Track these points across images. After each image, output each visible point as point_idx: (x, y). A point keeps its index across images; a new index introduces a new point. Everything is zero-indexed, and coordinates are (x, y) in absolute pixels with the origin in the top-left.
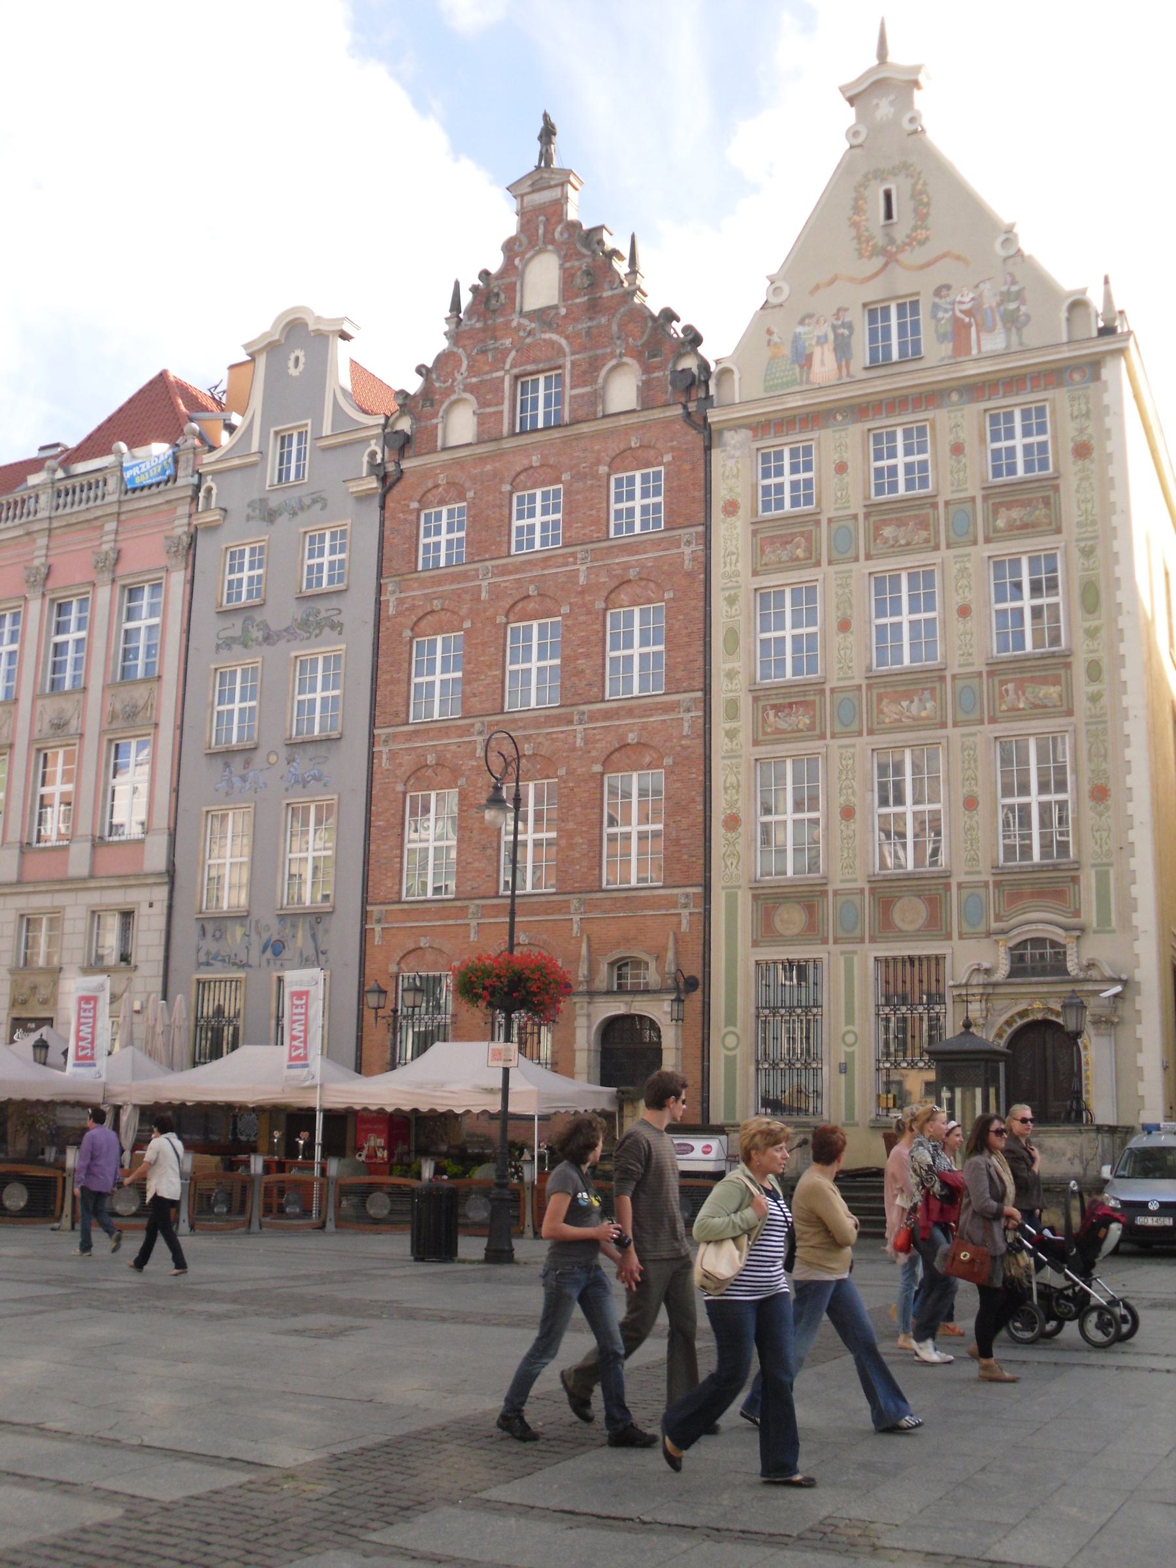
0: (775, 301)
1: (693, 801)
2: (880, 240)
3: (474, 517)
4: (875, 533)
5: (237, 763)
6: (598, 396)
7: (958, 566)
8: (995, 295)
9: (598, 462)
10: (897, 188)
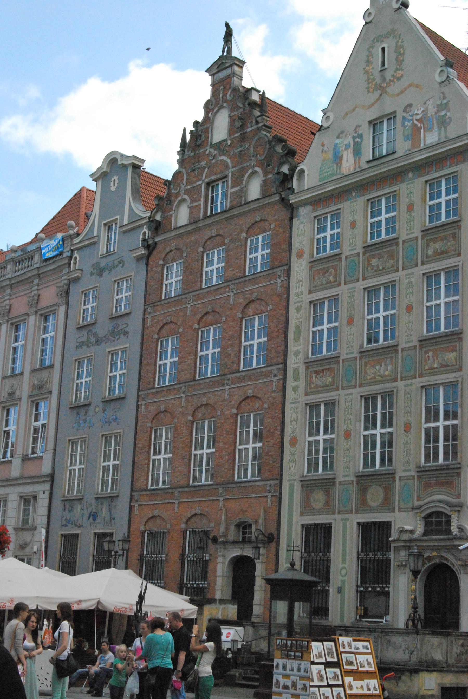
2: (378, 80)
4: (368, 265)
6: (243, 192)
7: (407, 281)
8: (434, 107)
9: (242, 231)
10: (388, 47)
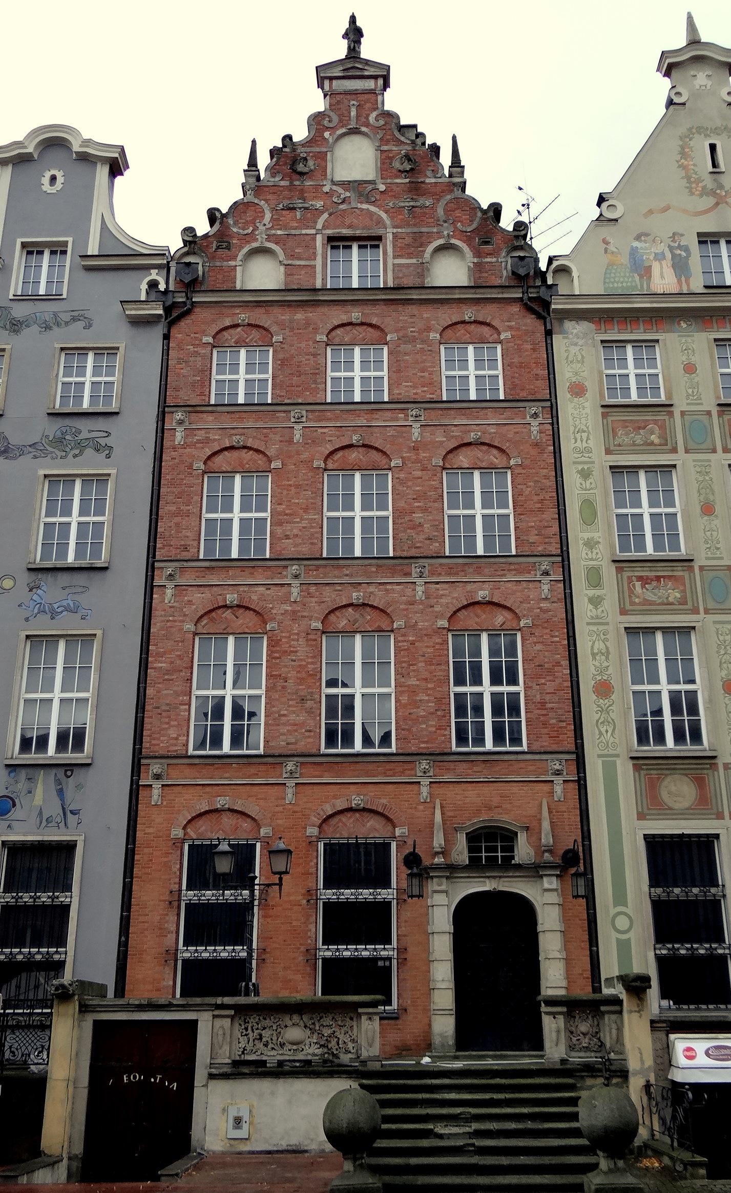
1: (558, 664)
6: (423, 269)
9: (429, 329)
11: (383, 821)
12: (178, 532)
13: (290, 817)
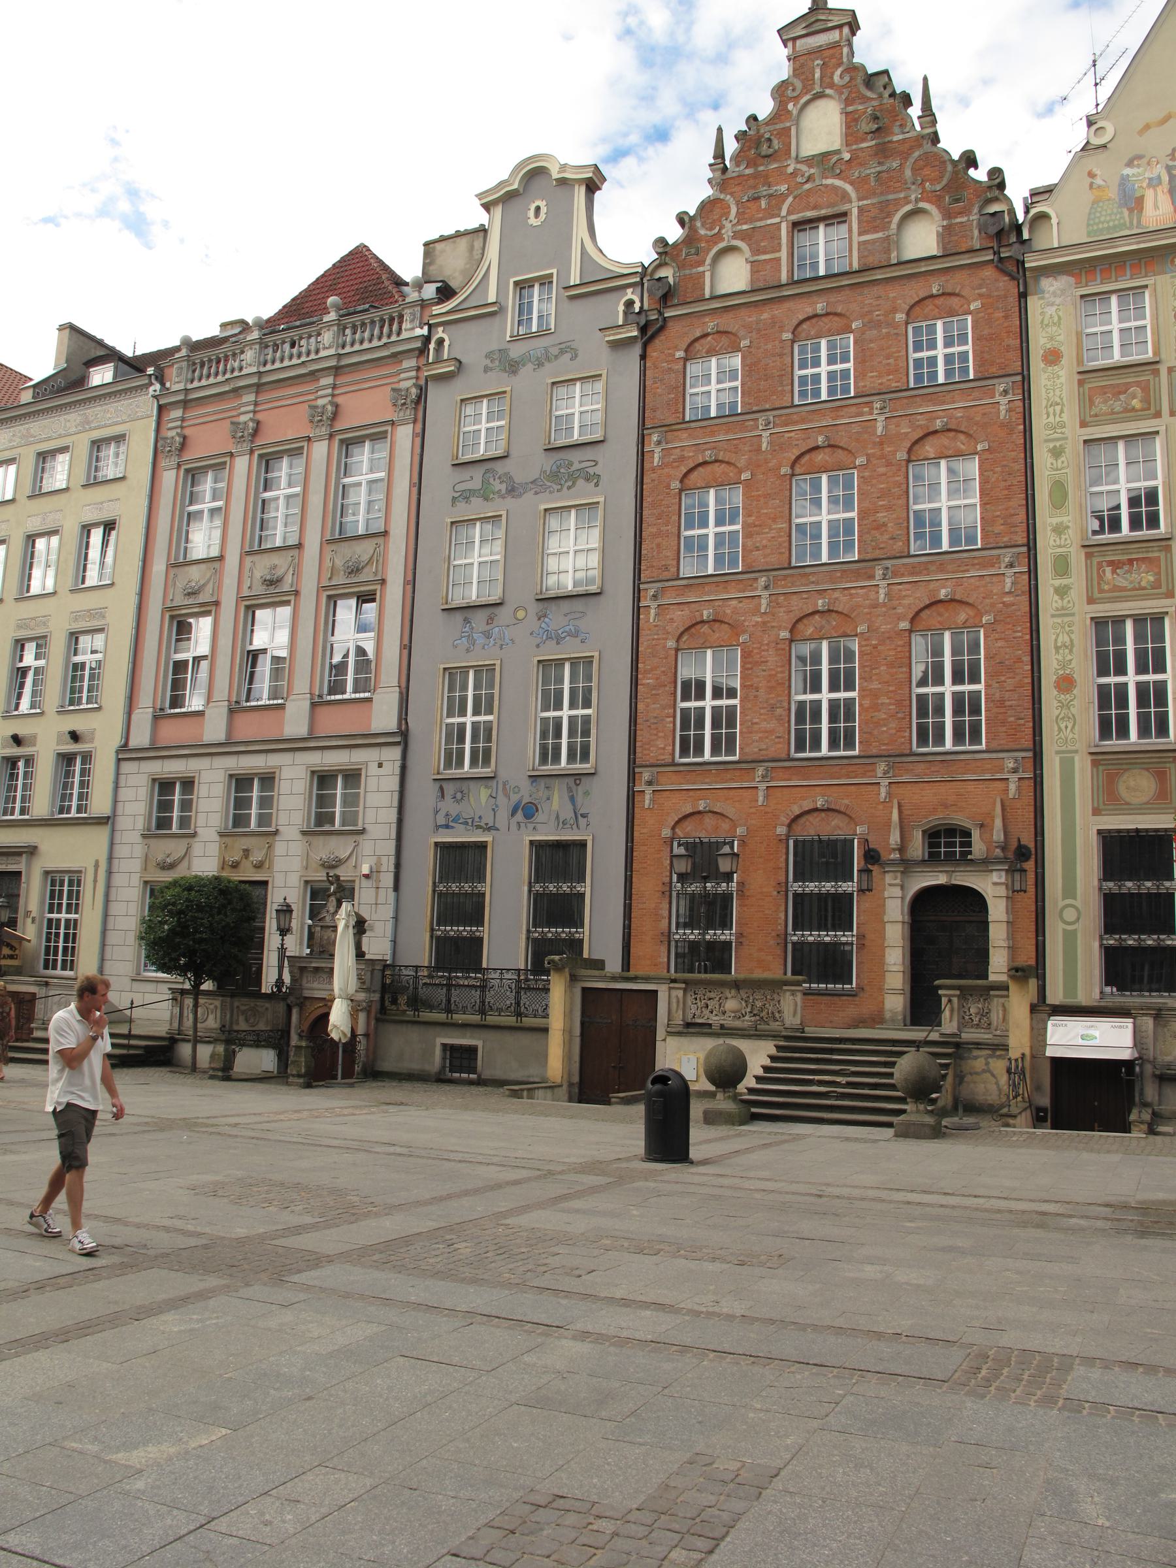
0: (1096, 141)
1: (1019, 660)
3: (750, 366)
5: (479, 618)
6: (891, 243)
9: (894, 310)
11: (847, 819)
12: (658, 553)
13: (756, 820)
